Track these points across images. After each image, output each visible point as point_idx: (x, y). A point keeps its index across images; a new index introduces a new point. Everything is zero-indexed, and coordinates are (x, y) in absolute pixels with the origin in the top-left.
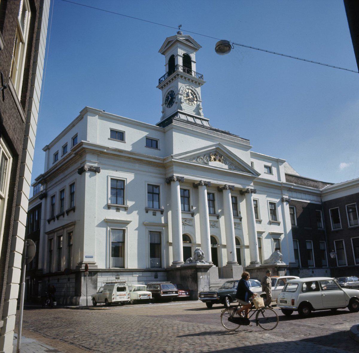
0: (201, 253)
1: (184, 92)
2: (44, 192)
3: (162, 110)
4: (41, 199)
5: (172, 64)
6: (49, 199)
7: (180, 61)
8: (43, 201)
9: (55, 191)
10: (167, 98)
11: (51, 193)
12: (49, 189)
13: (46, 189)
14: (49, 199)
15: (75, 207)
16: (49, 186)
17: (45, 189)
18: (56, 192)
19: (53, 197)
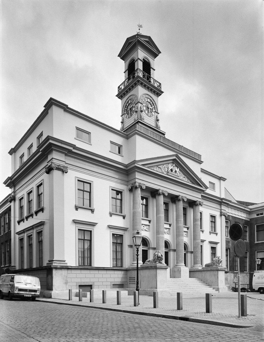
0: (160, 255)
1: (144, 101)
2: (13, 194)
3: (121, 121)
4: (11, 202)
5: (131, 69)
6: (17, 202)
7: (140, 65)
8: (12, 204)
9: (22, 193)
10: (125, 107)
11: (18, 196)
12: (17, 192)
13: (14, 192)
14: (17, 202)
15: (43, 207)
16: (17, 189)
17: (13, 192)
18: (24, 194)
19: (21, 199)
